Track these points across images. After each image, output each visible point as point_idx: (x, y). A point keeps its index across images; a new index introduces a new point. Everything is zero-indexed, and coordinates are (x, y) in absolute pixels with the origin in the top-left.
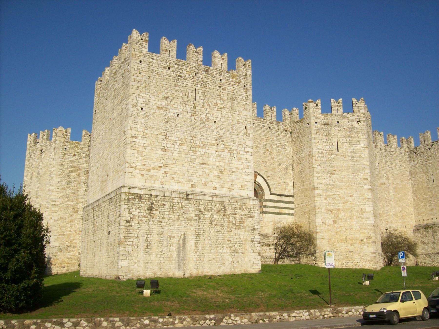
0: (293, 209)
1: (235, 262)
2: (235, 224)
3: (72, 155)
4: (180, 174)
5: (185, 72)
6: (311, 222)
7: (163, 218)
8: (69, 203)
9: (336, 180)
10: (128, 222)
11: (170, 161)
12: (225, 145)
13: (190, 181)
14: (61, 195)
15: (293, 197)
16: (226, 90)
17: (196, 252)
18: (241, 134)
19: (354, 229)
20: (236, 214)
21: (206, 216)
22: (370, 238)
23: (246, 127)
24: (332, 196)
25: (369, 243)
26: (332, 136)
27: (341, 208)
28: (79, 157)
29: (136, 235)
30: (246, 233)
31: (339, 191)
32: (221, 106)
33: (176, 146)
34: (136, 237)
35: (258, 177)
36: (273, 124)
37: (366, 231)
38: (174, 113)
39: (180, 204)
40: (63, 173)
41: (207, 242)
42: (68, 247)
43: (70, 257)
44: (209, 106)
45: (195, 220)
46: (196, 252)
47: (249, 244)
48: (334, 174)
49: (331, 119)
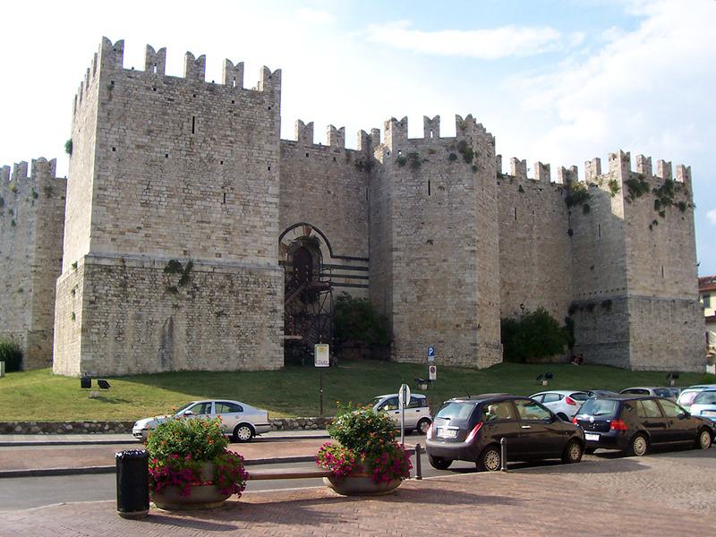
0: (367, 278)
1: (246, 355)
2: (246, 304)
3: (59, 198)
5: (177, 93)
7: (142, 297)
10: (92, 302)
11: (153, 220)
13: (182, 246)
14: (43, 257)
15: (367, 260)
17: (188, 342)
18: (262, 178)
20: (248, 290)
21: (204, 294)
22: (469, 322)
23: (269, 169)
25: (468, 330)
29: (103, 321)
30: (263, 316)
32: (233, 139)
34: (103, 323)
39: (166, 278)
40: (46, 225)
41: (204, 328)
44: (214, 139)
45: (188, 299)
46: (188, 342)
47: (266, 331)
48: (421, 228)
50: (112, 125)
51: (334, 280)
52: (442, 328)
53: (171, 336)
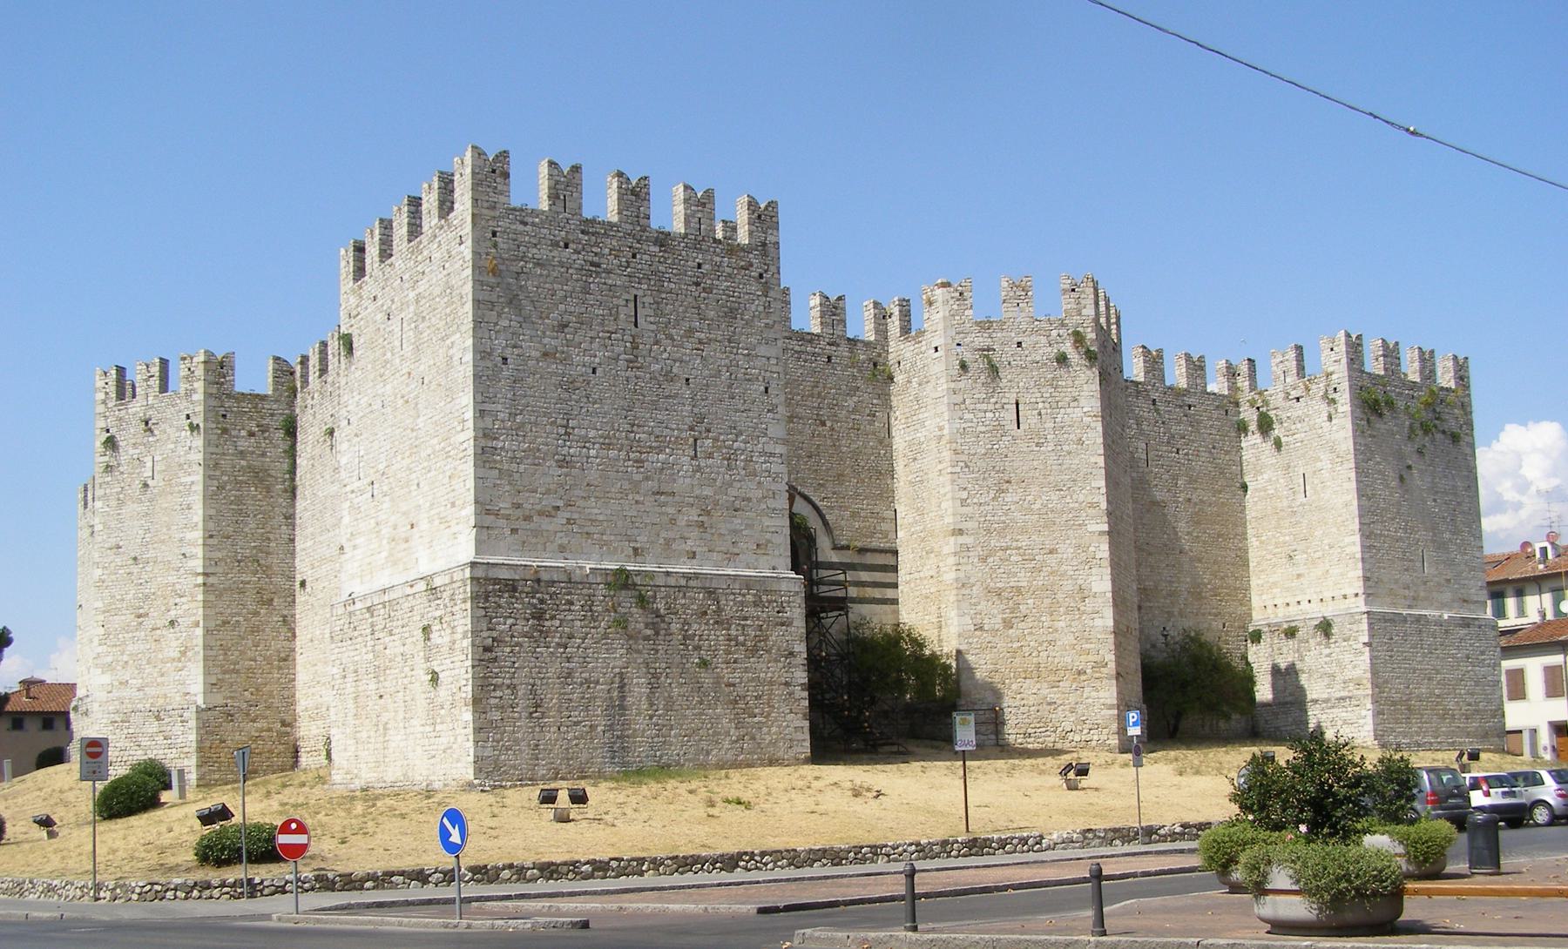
3: (243, 433)
4: (605, 524)
6: (943, 623)
7: (571, 637)
8: (245, 578)
9: (1013, 507)
10: (487, 649)
12: (716, 440)
16: (714, 291)
17: (651, 718)
19: (1058, 643)
20: (746, 619)
23: (766, 392)
24: (1000, 553)
26: (1001, 385)
27: (1025, 584)
28: (265, 439)
29: (508, 682)
31: (1019, 537)
33: (592, 452)
34: (508, 687)
35: (798, 498)
36: (838, 345)
37: (1092, 646)
38: (584, 366)
40: (220, 488)
42: (251, 706)
43: (257, 734)
45: (647, 638)
49: (999, 335)
50: (499, 315)
51: (853, 592)
52: (1052, 678)
53: (622, 707)
